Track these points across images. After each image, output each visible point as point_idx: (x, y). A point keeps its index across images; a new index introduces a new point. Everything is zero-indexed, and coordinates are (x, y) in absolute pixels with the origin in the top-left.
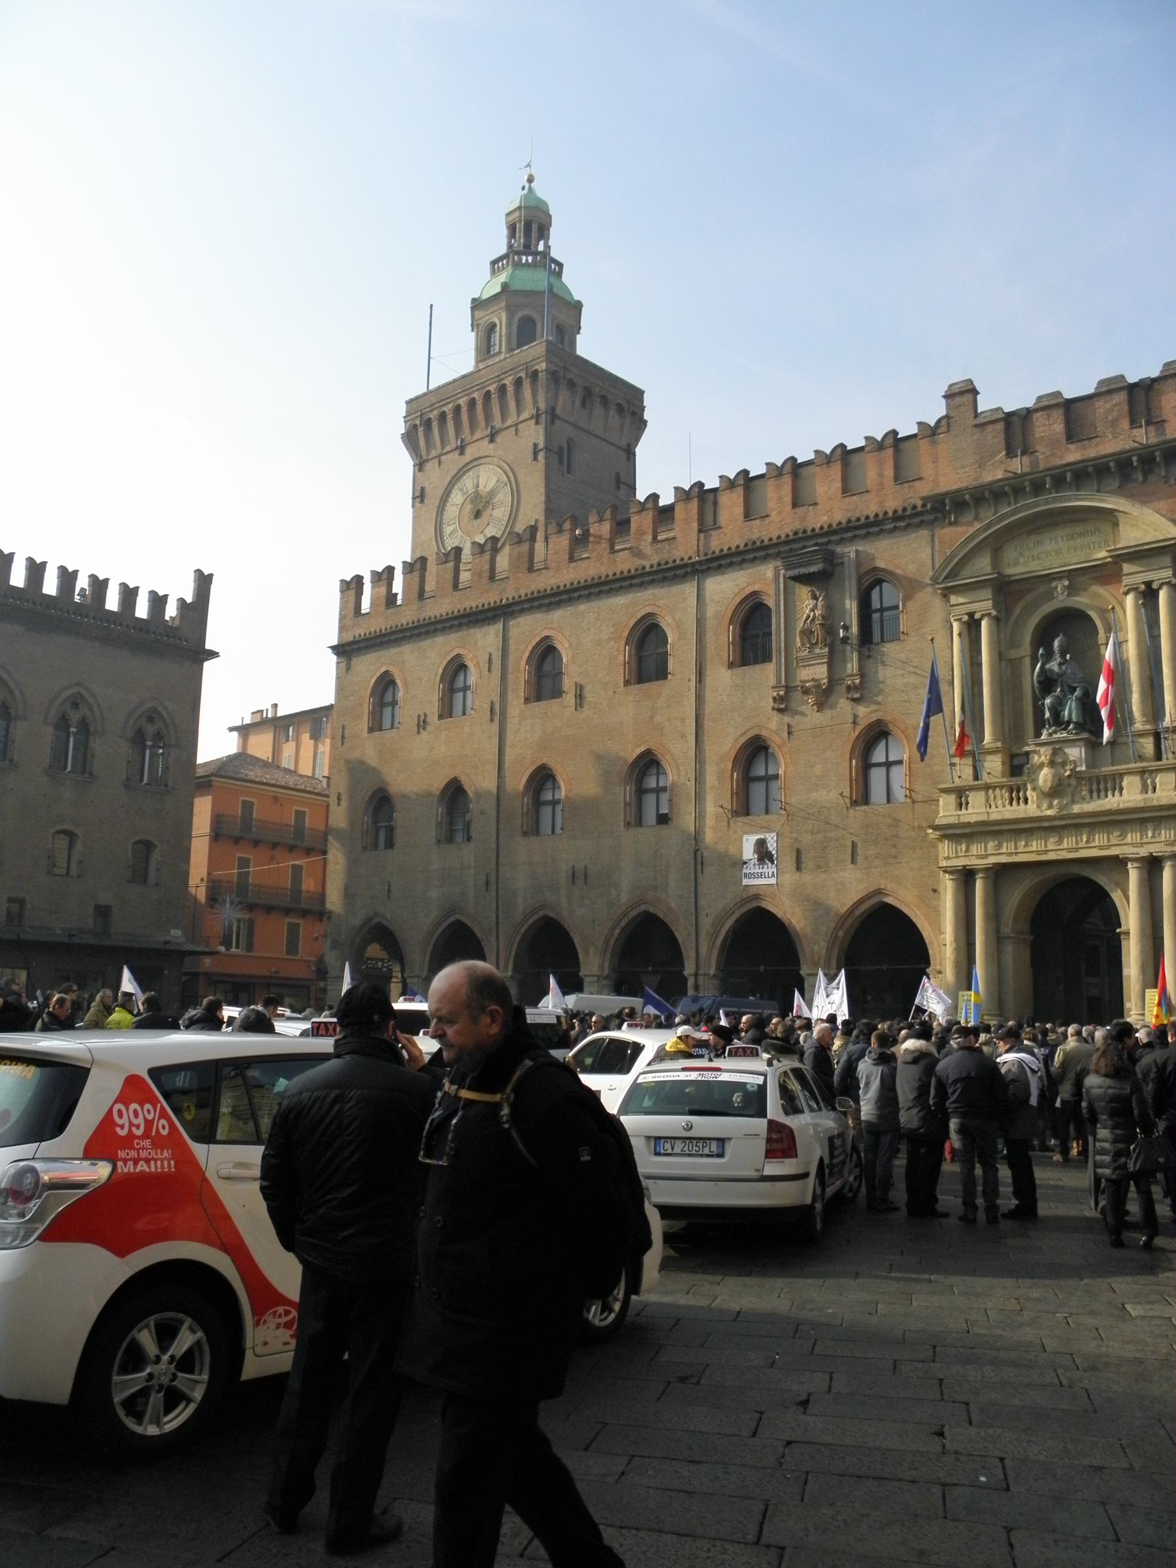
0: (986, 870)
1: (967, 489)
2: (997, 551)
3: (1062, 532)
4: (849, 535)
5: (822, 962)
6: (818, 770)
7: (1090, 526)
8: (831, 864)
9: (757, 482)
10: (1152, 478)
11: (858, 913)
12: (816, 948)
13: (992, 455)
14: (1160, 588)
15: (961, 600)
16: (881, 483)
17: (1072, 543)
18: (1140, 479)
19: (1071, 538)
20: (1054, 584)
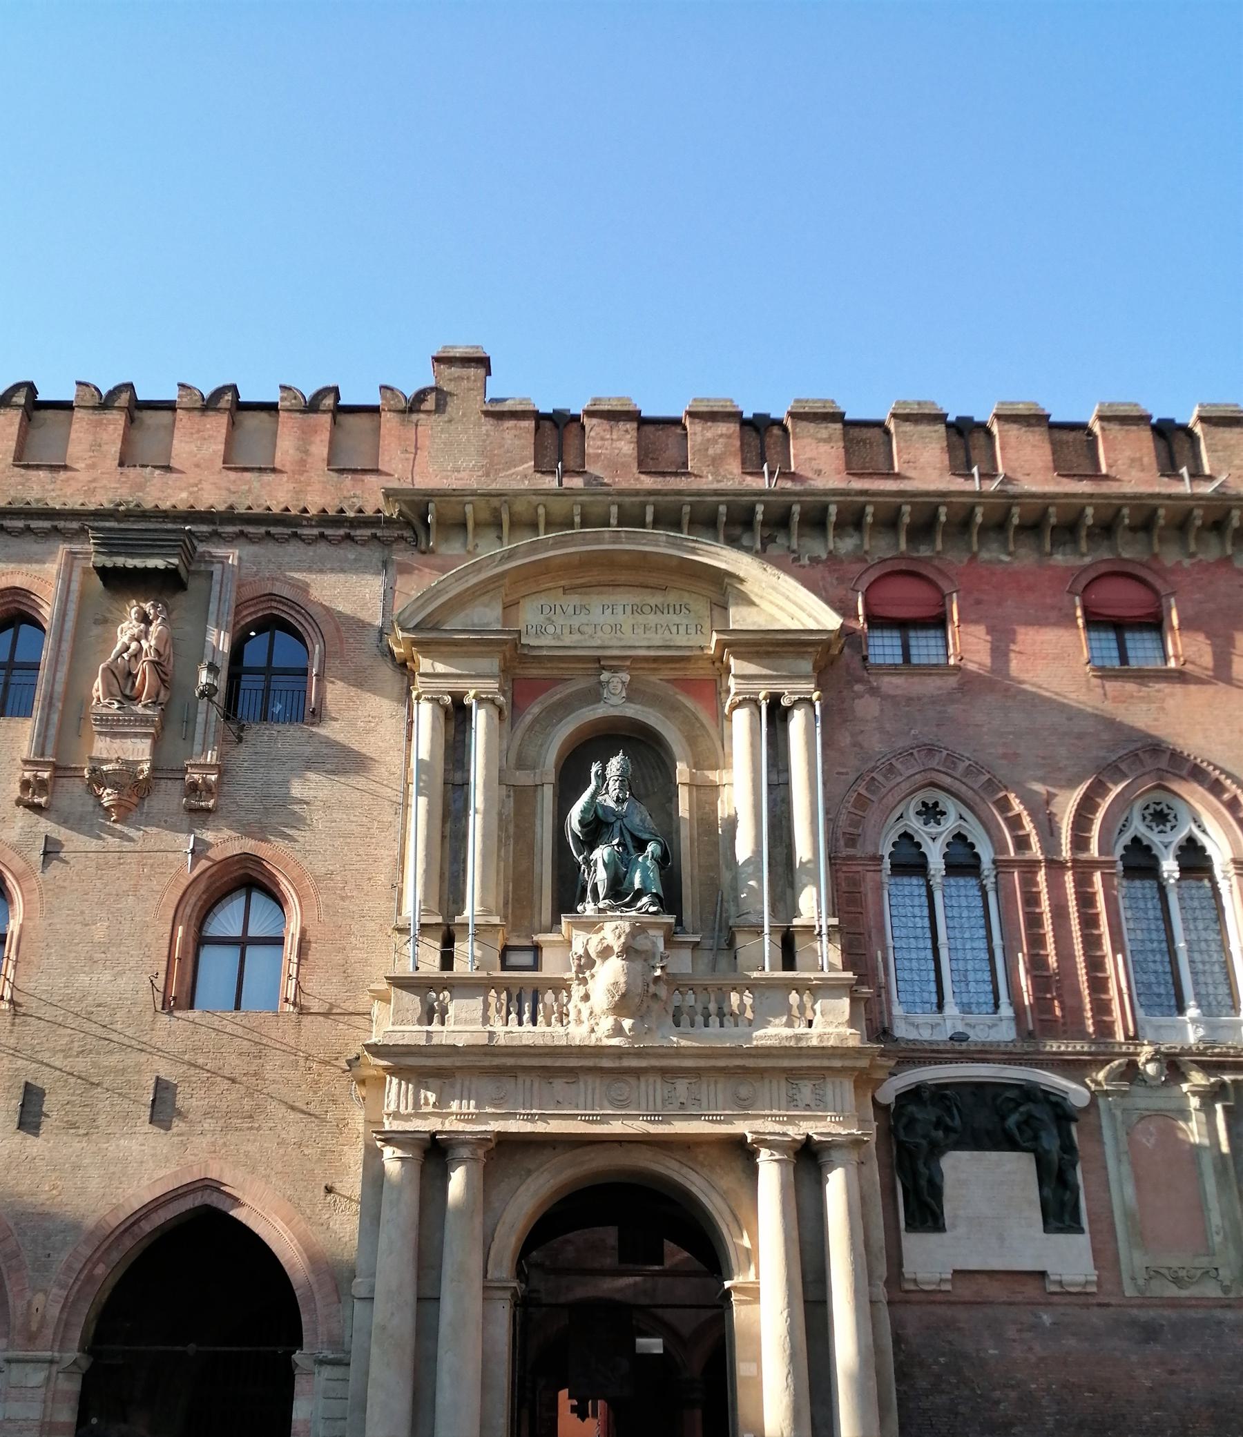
0: (481, 1141)
1: (474, 493)
2: (509, 606)
3: (625, 598)
4: (230, 529)
5: (49, 1332)
6: (99, 931)
7: (672, 598)
8: (101, 1121)
9: (49, 414)
10: (773, 550)
11: (147, 1227)
12: (39, 1300)
13: (511, 464)
14: (795, 704)
15: (441, 668)
16: (302, 462)
17: (640, 619)
18: (758, 546)
19: (637, 610)
20: (605, 676)
